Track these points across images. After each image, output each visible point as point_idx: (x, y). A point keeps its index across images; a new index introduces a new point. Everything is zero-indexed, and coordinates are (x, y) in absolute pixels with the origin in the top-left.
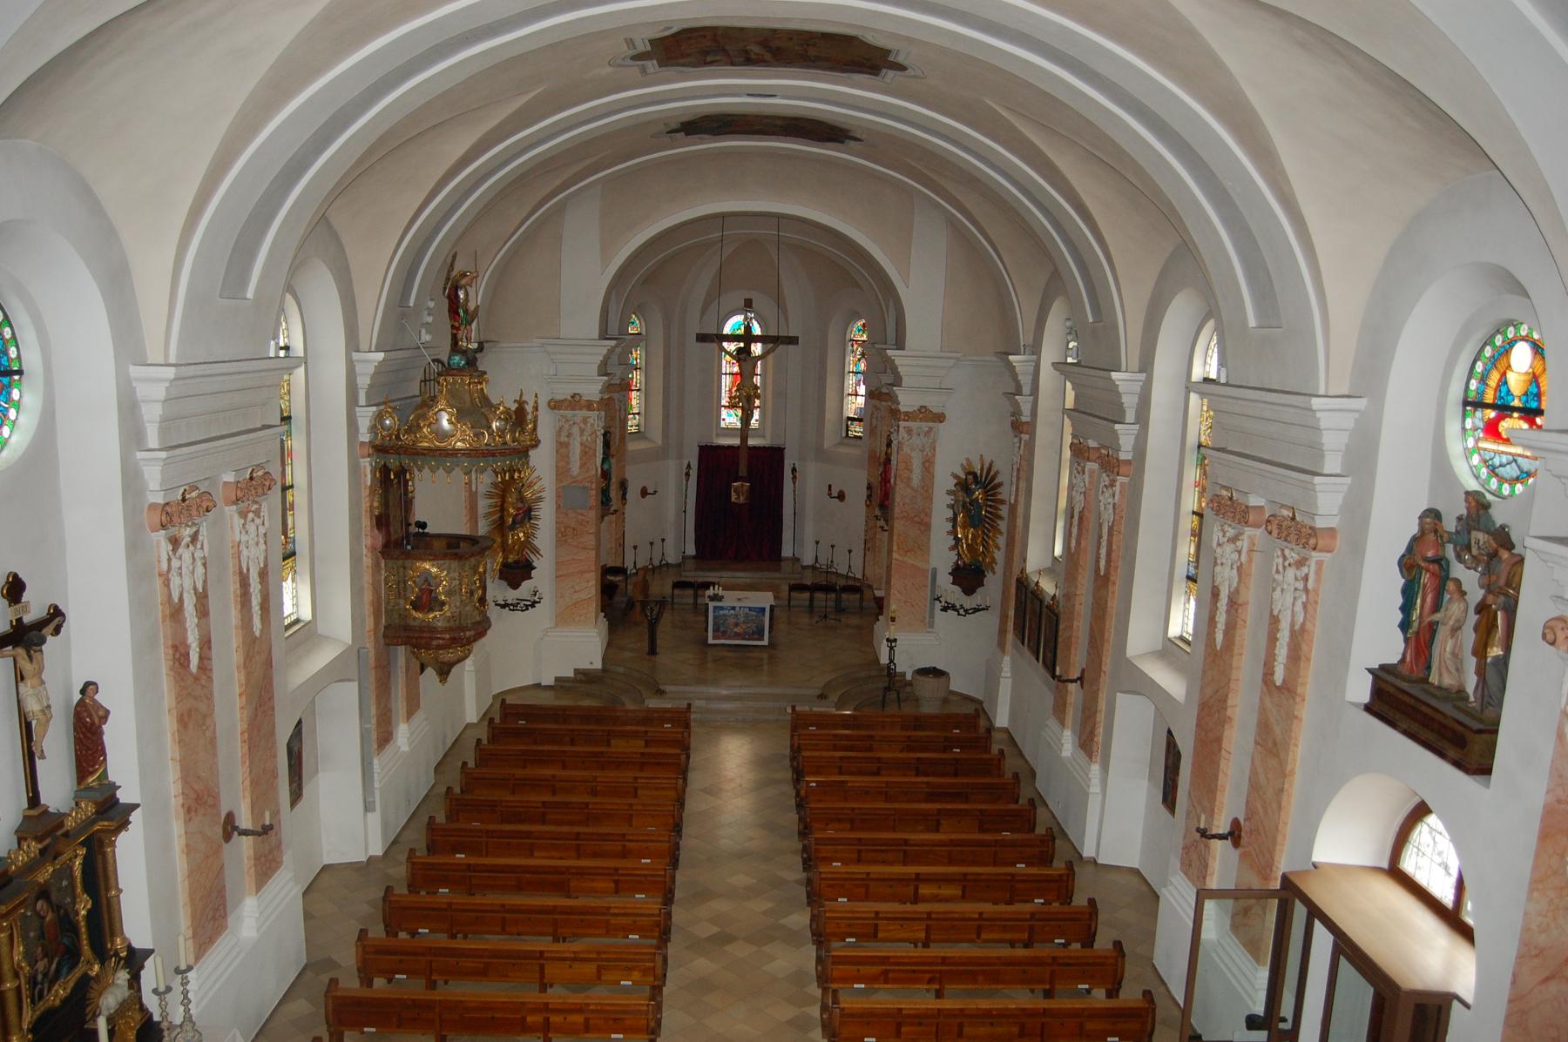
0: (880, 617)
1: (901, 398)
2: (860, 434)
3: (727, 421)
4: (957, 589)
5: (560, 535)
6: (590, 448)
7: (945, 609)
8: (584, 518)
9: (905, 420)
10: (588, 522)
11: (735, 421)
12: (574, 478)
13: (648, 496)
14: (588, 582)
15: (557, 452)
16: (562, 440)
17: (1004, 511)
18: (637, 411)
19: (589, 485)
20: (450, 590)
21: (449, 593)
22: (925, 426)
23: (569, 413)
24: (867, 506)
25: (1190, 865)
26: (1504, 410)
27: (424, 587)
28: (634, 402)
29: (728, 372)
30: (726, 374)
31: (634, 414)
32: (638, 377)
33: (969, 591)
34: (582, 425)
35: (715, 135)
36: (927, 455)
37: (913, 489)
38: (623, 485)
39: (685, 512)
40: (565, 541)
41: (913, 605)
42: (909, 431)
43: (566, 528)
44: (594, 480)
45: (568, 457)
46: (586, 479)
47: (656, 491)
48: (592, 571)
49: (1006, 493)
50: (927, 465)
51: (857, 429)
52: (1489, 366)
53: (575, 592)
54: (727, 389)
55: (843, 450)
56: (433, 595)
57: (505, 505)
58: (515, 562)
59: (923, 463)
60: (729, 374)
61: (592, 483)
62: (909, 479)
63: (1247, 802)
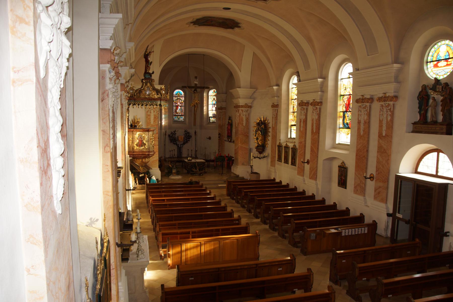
0: (233, 164)
3: (175, 119)
6: (156, 116)
9: (241, 108)
10: (156, 138)
12: (152, 125)
15: (147, 117)
16: (148, 114)
17: (270, 130)
19: (156, 127)
20: (147, 140)
22: (246, 109)
24: (219, 140)
25: (357, 190)
26: (439, 61)
30: (174, 106)
33: (261, 153)
35: (199, 26)
37: (244, 126)
39: (165, 145)
41: (245, 159)
42: (242, 111)
45: (150, 119)
46: (155, 125)
49: (270, 125)
51: (212, 120)
52: (434, 52)
54: (175, 110)
56: (143, 142)
61: (157, 126)
62: (243, 124)
63: (376, 167)
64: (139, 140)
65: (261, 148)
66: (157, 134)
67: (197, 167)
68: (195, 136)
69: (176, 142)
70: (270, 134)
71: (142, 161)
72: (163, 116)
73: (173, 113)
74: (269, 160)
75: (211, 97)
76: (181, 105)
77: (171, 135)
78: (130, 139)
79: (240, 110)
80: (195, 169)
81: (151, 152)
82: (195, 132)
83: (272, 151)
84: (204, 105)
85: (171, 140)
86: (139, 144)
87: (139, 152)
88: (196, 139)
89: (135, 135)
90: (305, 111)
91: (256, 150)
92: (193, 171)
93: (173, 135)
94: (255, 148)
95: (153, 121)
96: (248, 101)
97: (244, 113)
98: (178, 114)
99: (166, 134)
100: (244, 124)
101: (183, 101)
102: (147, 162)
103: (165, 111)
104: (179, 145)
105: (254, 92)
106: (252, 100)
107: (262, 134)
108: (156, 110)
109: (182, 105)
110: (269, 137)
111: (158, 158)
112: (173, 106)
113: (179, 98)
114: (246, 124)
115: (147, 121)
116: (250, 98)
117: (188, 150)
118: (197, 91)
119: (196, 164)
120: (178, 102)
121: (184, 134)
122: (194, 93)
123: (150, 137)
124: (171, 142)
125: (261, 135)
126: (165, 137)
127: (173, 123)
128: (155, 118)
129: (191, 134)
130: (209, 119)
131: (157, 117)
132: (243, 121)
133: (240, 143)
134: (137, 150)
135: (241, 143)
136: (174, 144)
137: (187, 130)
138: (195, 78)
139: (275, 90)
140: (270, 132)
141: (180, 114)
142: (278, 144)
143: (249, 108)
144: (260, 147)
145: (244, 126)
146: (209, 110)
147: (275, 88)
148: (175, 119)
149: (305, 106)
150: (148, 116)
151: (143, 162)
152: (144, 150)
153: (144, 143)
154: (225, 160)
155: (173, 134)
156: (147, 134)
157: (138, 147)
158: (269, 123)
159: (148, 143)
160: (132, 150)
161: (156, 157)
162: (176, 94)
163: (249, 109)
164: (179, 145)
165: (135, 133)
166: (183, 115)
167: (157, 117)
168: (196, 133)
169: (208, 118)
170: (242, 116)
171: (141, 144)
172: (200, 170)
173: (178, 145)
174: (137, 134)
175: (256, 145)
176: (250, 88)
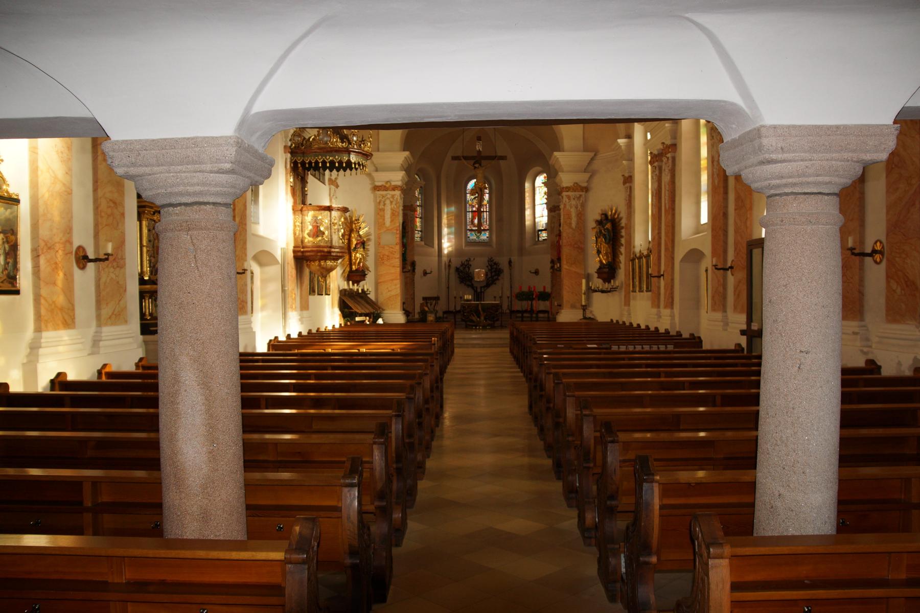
1: (563, 179)
2: (546, 238)
3: (471, 238)
4: (600, 281)
5: (380, 260)
6: (396, 211)
7: (595, 291)
10: (395, 252)
11: (475, 238)
13: (428, 275)
14: (396, 285)
15: (378, 214)
16: (381, 207)
17: (623, 233)
19: (396, 231)
20: (328, 226)
21: (327, 228)
22: (577, 194)
23: (384, 193)
27: (314, 224)
28: (418, 224)
29: (470, 210)
30: (469, 212)
31: (418, 231)
34: (391, 199)
37: (572, 228)
38: (413, 264)
39: (448, 288)
40: (383, 263)
42: (569, 197)
44: (398, 229)
45: (384, 216)
46: (393, 228)
47: (431, 272)
48: (397, 279)
53: (389, 291)
55: (536, 246)
56: (318, 229)
57: (351, 238)
58: (356, 270)
61: (397, 230)
62: (570, 224)
64: (313, 226)
65: (608, 272)
66: (397, 244)
67: (482, 313)
68: (510, 269)
70: (623, 241)
71: (320, 265)
72: (445, 231)
74: (623, 293)
75: (541, 189)
77: (461, 268)
78: (298, 224)
79: (564, 197)
80: (476, 317)
81: (335, 248)
82: (510, 262)
83: (625, 275)
84: (527, 206)
86: (312, 233)
87: (313, 247)
88: (511, 276)
89: (306, 218)
90: (657, 172)
91: (596, 275)
92: (472, 321)
93: (464, 268)
94: (596, 272)
95: (389, 220)
96: (581, 178)
97: (573, 202)
99: (449, 266)
102: (329, 267)
103: (448, 220)
104: (477, 287)
105: (592, 159)
106: (586, 176)
107: (607, 241)
108: (395, 199)
109: (485, 210)
110: (622, 247)
111: (399, 291)
112: (466, 212)
114: (578, 223)
116: (585, 171)
117: (495, 297)
118: (480, 165)
119: (480, 309)
121: (487, 267)
122: (475, 169)
123: (333, 220)
125: (605, 243)
126: (449, 271)
127: (465, 246)
128: (393, 214)
129: (500, 267)
130: (537, 234)
131: (396, 214)
132: (569, 217)
133: (565, 262)
134: (310, 244)
135: (567, 263)
136: (468, 286)
137: (493, 258)
138: (478, 140)
139: (623, 147)
140: (622, 237)
142: (632, 256)
143: (583, 191)
144: (605, 268)
145: (574, 227)
146: (536, 216)
147: (622, 141)
148: (471, 238)
149: (657, 161)
150: (379, 212)
151: (322, 266)
152: (322, 244)
153: (321, 231)
154: (534, 297)
155: (464, 266)
156: (327, 215)
157: (311, 239)
158: (621, 219)
159: (330, 231)
160: (300, 244)
163: (583, 193)
164: (477, 287)
165: (305, 213)
166: (486, 228)
167: (396, 214)
168: (512, 264)
169: (536, 232)
171: (317, 232)
172: (485, 319)
173: (475, 288)
174: (309, 216)
175: (598, 266)
176: (584, 151)
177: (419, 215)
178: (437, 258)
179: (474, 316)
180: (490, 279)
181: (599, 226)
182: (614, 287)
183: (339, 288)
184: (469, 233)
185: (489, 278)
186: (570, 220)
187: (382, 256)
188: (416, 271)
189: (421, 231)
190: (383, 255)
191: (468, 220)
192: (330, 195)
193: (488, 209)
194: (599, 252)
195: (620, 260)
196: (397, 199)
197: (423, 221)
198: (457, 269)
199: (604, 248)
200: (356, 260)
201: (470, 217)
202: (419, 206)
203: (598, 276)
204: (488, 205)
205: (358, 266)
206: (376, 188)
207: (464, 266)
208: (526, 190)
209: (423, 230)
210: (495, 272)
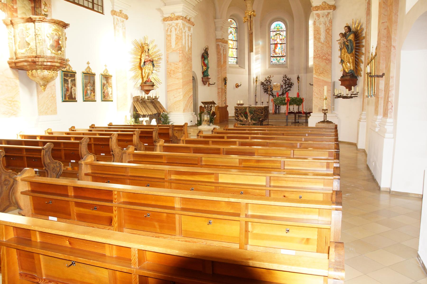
3: (273, 62)
4: (344, 88)
5: (168, 74)
8: (177, 66)
10: (179, 68)
11: (276, 62)
14: (179, 93)
15: (167, 39)
16: (168, 34)
18: (236, 57)
19: (179, 51)
22: (326, 12)
29: (273, 43)
30: (272, 44)
32: (236, 44)
36: (328, 26)
37: (321, 43)
39: (256, 96)
43: (170, 71)
44: (181, 49)
45: (171, 40)
46: (178, 49)
48: (180, 88)
50: (328, 31)
54: (273, 50)
59: (326, 30)
60: (274, 44)
61: (180, 51)
62: (320, 38)
67: (248, 114)
68: (298, 83)
69: (272, 92)
73: (270, 53)
76: (281, 42)
82: (298, 78)
85: (264, 89)
88: (299, 87)
91: (340, 82)
93: (267, 83)
97: (322, 20)
98: (277, 54)
99: (256, 81)
100: (321, 40)
101: (283, 37)
109: (283, 43)
113: (278, 32)
115: (167, 45)
119: (247, 111)
120: (277, 38)
121: (282, 81)
124: (265, 92)
131: (179, 38)
135: (316, 72)
141: (281, 55)
143: (331, 9)
144: (347, 76)
145: (323, 41)
150: (168, 37)
155: (267, 81)
161: (179, 95)
162: (274, 29)
163: (331, 11)
164: (275, 95)
166: (284, 55)
167: (179, 38)
168: (300, 79)
170: (319, 25)
172: (252, 119)
177: (235, 47)
178: (247, 76)
179: (242, 117)
180: (285, 90)
181: (343, 38)
182: (354, 93)
183: (132, 95)
184: (272, 59)
185: (284, 89)
186: (319, 35)
187: (169, 71)
188: (227, 84)
189: (237, 58)
190: (170, 71)
191: (272, 50)
192: (114, 24)
193: (285, 41)
194: (342, 62)
195: (361, 69)
196: (180, 26)
197: (238, 51)
198: (262, 84)
199: (350, 58)
200: (145, 75)
201: (273, 48)
202: (235, 41)
203: (341, 83)
204: (285, 39)
205: (147, 78)
206: (165, 19)
207: (267, 81)
208: (309, 26)
209: (238, 57)
210: (288, 84)
